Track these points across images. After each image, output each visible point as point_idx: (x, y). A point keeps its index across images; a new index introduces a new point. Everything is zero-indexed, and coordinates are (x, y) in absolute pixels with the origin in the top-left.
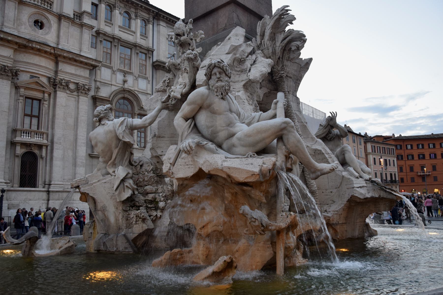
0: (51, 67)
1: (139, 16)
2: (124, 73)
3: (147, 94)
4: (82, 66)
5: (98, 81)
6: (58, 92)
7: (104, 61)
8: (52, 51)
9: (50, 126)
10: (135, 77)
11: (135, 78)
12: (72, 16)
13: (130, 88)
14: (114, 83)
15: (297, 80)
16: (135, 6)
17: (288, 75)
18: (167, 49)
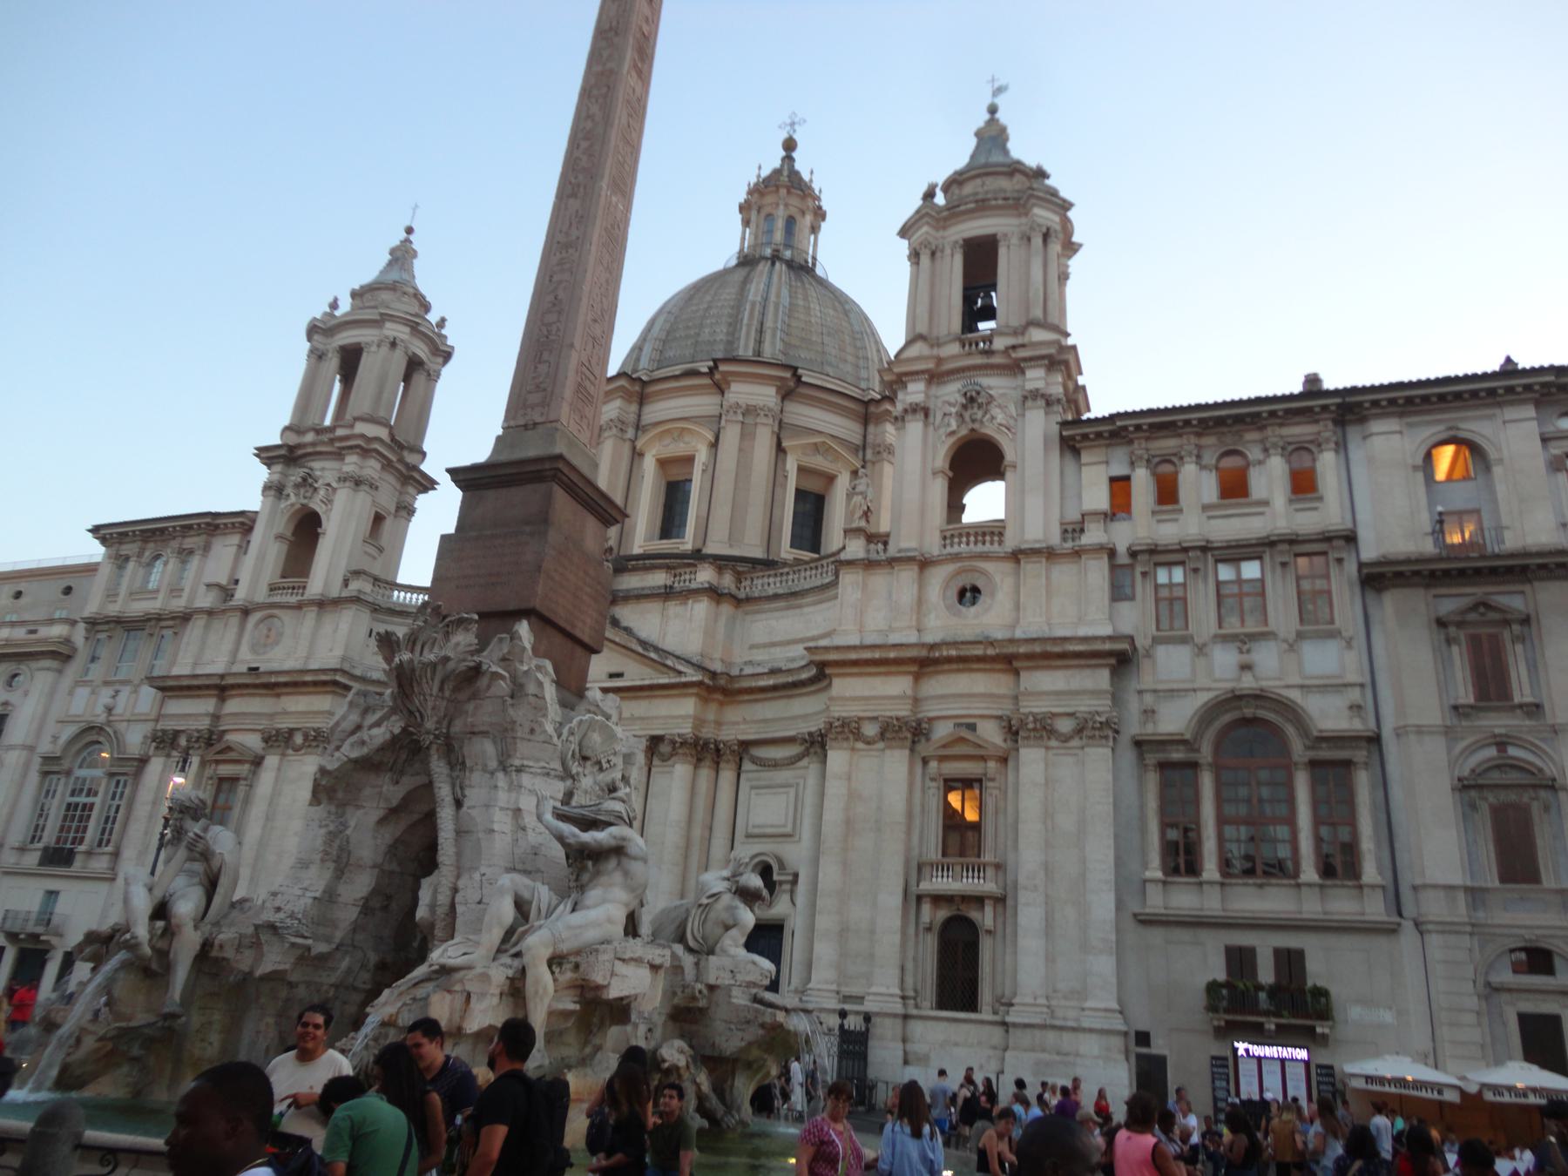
0: (1003, 691)
1: (1275, 446)
2: (1238, 644)
3: (1345, 685)
4: (1083, 662)
5: (1147, 691)
6: (1023, 751)
7: (1165, 624)
8: (990, 652)
9: (1009, 843)
10: (1285, 641)
11: (1285, 646)
12: (1055, 539)
13: (1264, 684)
14: (1202, 681)
15: (506, 730)
16: (1252, 423)
17: (476, 730)
18: (1423, 501)
